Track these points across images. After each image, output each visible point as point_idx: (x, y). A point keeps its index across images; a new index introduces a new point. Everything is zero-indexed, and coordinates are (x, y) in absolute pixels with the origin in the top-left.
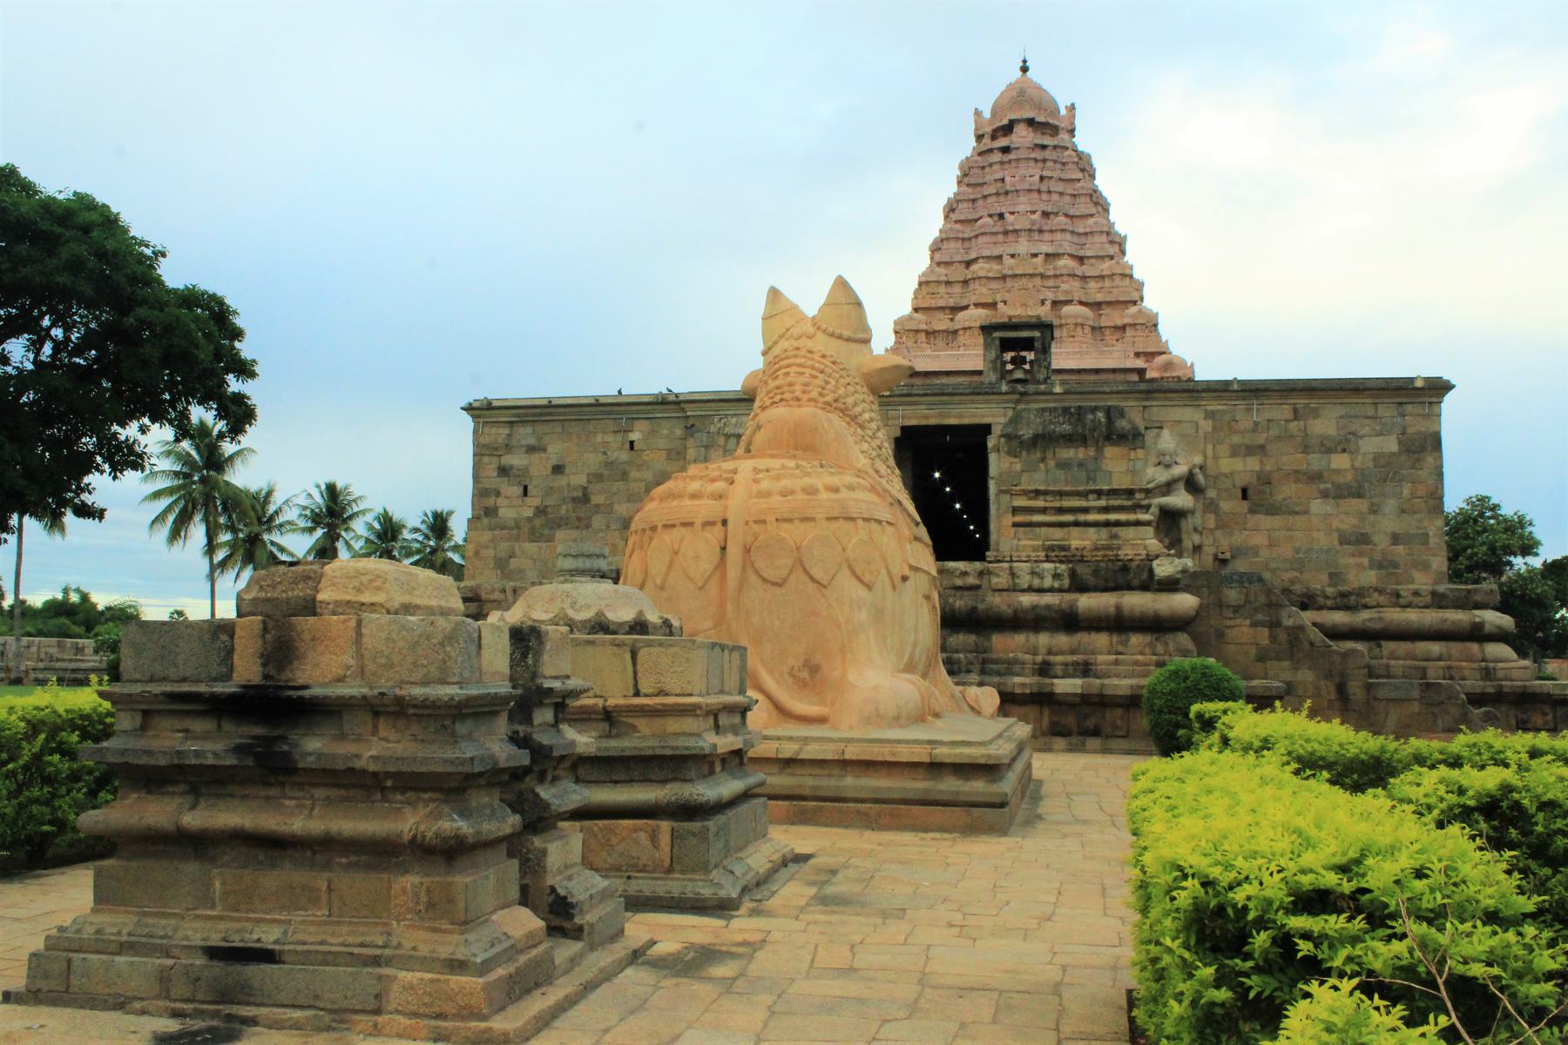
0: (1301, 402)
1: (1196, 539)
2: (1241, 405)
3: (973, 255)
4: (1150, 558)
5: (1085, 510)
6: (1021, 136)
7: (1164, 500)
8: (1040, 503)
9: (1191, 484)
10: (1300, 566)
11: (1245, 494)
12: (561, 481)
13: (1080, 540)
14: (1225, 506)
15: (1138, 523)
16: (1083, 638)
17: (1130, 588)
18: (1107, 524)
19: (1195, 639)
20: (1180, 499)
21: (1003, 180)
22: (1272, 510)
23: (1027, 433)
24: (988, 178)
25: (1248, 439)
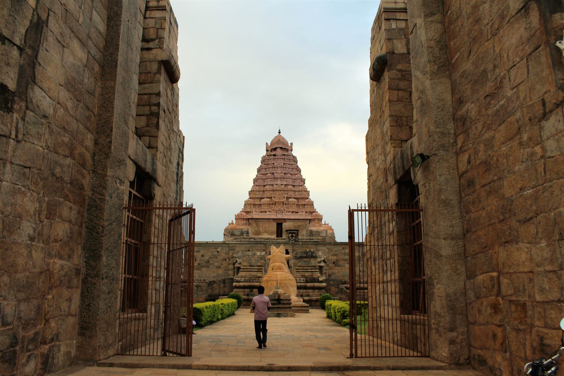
0: (344, 246)
1: (325, 271)
2: (333, 247)
3: (266, 184)
4: (318, 277)
5: (308, 269)
6: (279, 152)
7: (320, 264)
8: (300, 268)
9: (324, 261)
10: (344, 276)
11: (334, 263)
12: (203, 258)
13: (307, 274)
14: (330, 265)
15: (317, 271)
16: (308, 290)
17: (315, 282)
18: (312, 271)
19: (325, 290)
20: (322, 264)
21: (274, 164)
22: (339, 266)
23: (298, 256)
24: (270, 163)
25: (334, 253)
